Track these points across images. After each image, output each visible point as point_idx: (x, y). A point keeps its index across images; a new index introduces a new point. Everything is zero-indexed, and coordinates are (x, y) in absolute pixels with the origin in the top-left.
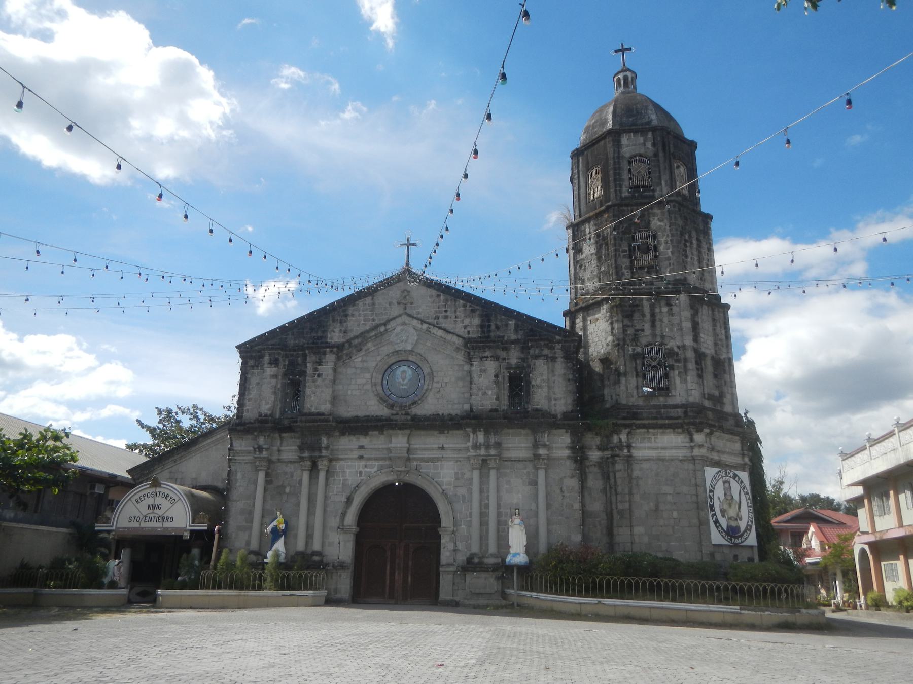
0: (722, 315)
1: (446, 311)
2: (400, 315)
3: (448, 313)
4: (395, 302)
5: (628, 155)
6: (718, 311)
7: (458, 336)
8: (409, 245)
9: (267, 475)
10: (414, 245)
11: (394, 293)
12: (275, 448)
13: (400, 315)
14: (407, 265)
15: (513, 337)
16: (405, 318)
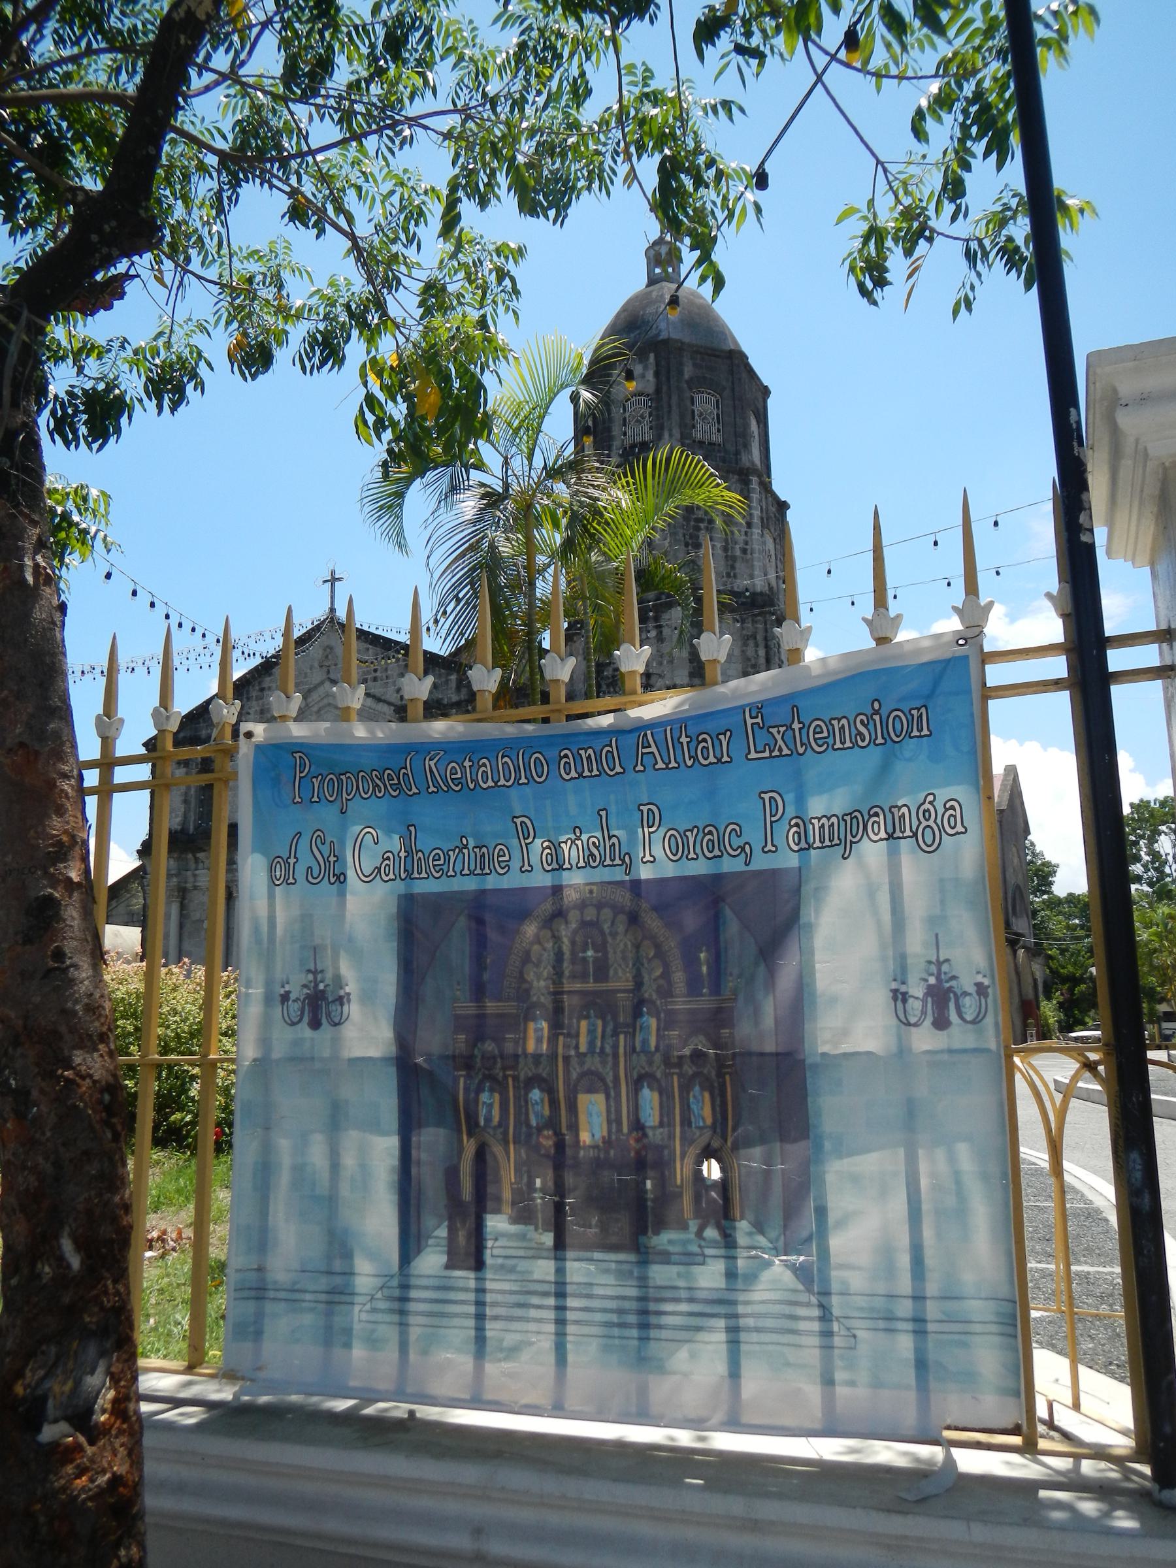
0: (760, 626)
1: (375, 671)
2: (322, 683)
3: (378, 674)
4: (316, 665)
5: (621, 397)
6: (754, 622)
7: (389, 704)
8: (333, 580)
9: (183, 907)
10: (339, 579)
11: (315, 650)
12: (189, 873)
13: (322, 683)
14: (332, 610)
15: (455, 698)
16: (327, 684)
